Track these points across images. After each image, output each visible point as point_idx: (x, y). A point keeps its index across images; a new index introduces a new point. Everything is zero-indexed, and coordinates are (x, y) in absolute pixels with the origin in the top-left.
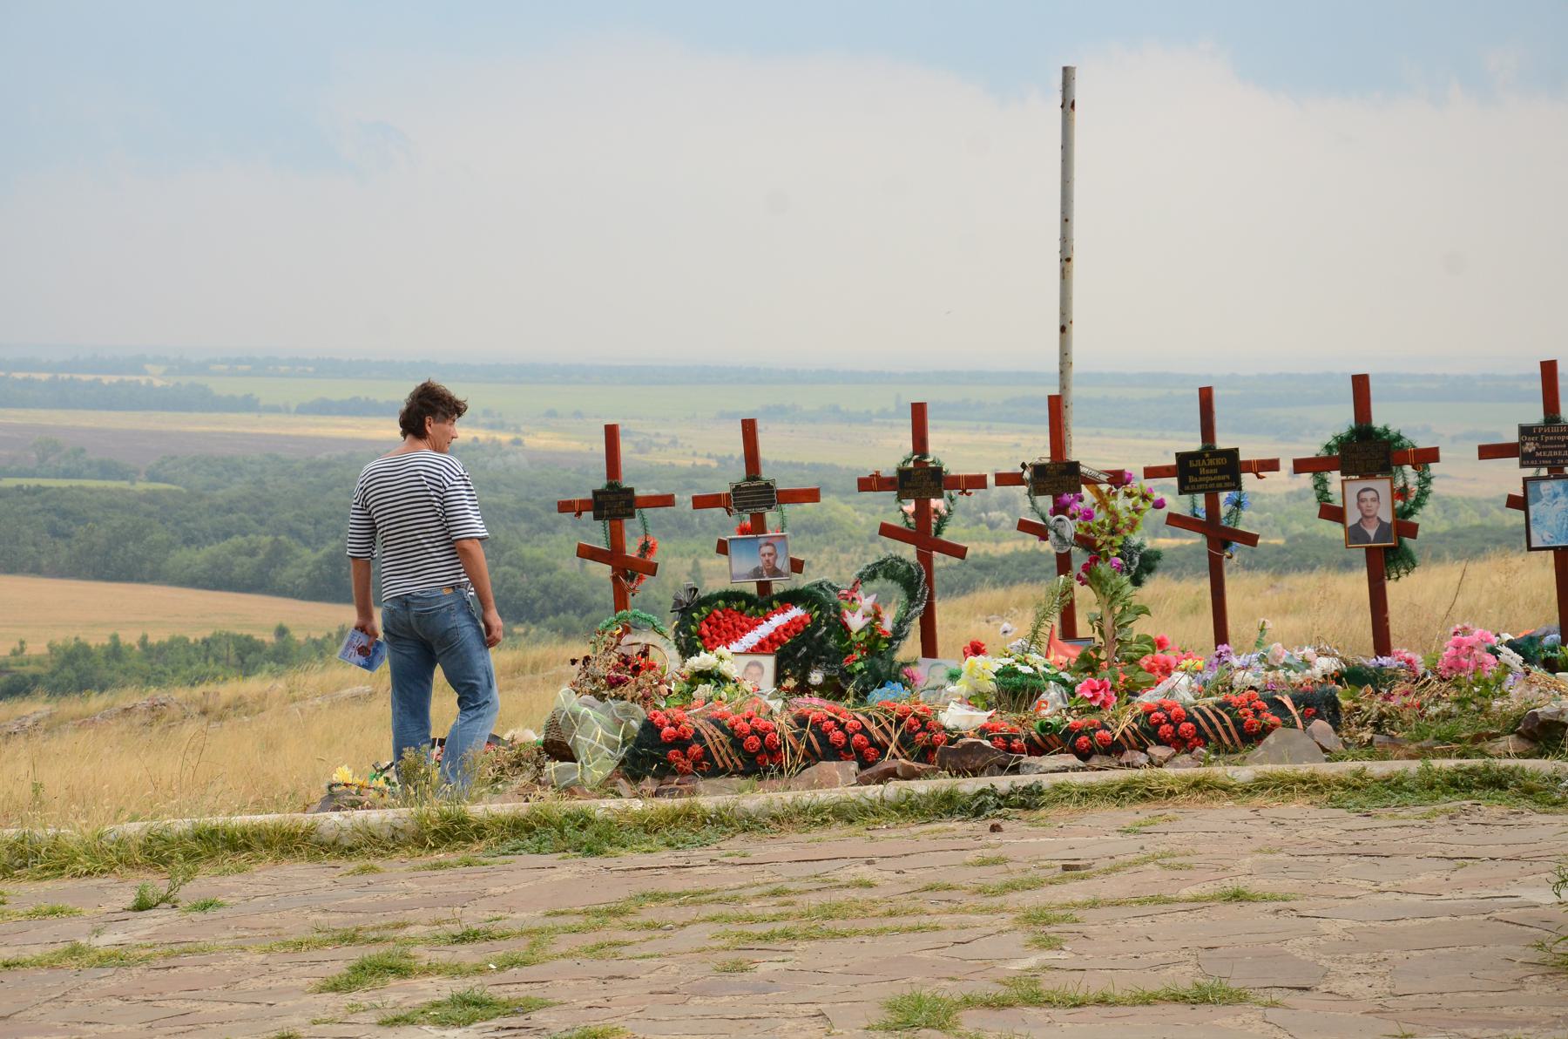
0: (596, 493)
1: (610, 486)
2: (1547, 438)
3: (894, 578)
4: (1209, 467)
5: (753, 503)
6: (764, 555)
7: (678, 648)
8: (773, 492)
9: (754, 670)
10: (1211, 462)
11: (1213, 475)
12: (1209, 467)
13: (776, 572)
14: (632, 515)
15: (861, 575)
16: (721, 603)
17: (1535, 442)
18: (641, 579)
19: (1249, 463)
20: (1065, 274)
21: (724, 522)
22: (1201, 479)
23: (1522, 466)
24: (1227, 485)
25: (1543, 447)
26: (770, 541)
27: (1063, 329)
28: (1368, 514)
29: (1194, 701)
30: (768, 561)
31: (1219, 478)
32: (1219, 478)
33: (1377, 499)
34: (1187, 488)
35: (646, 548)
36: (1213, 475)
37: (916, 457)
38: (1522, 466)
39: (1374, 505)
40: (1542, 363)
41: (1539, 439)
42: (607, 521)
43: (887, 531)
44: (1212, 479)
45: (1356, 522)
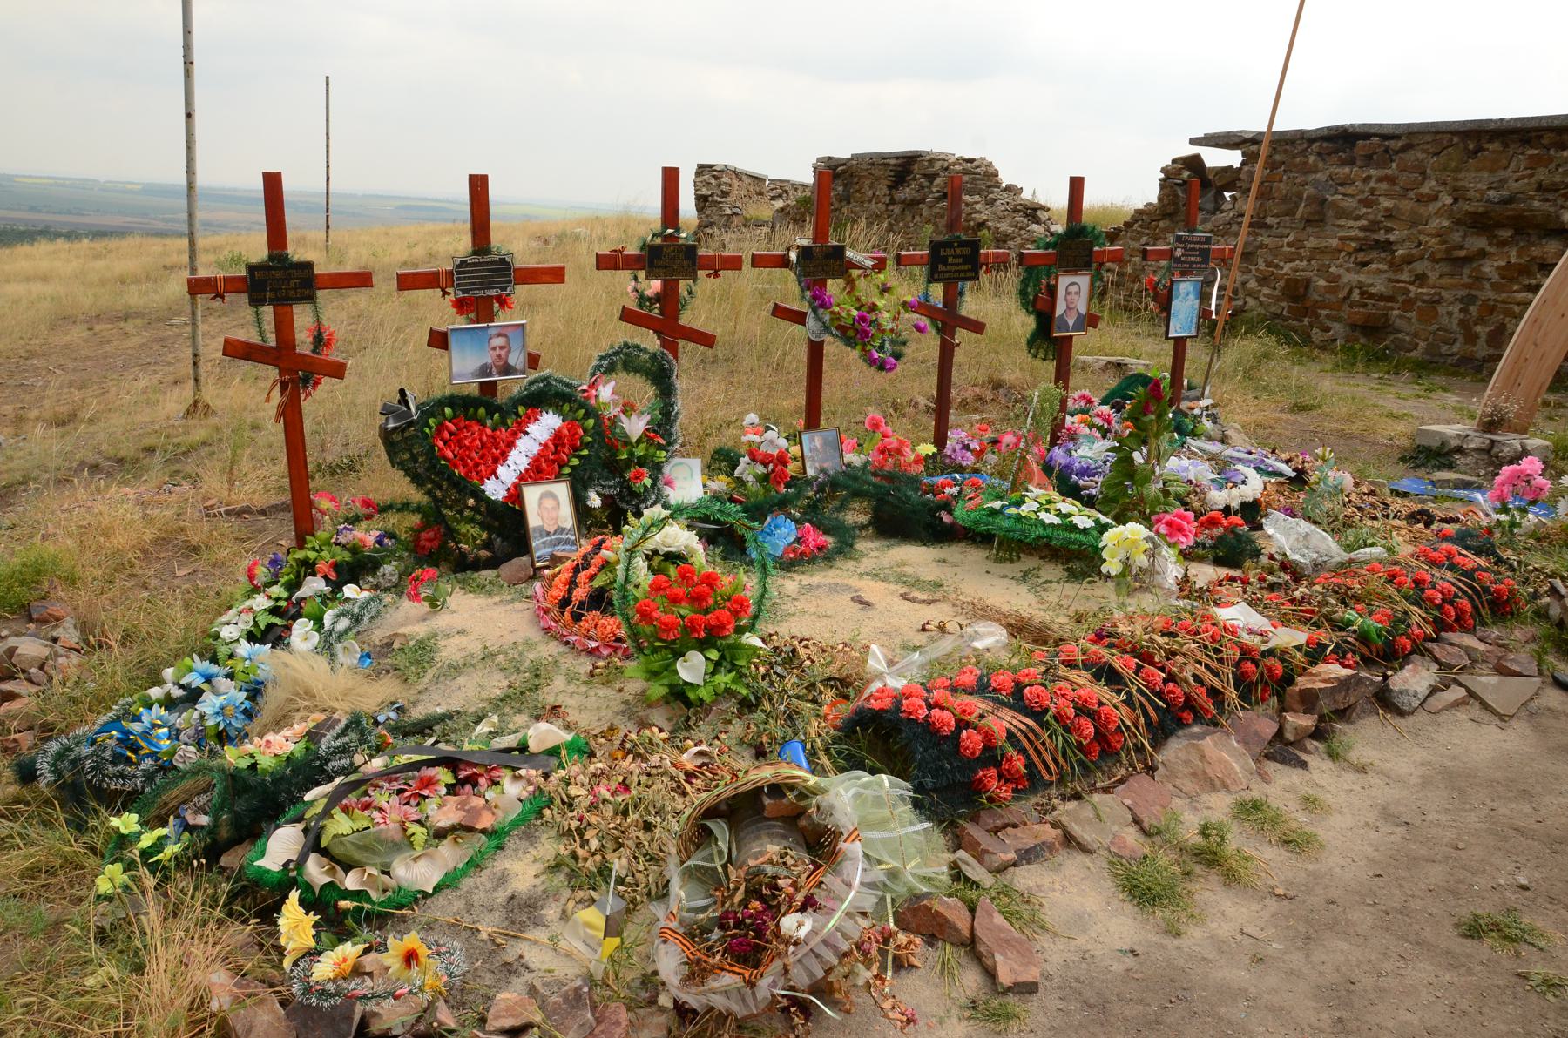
0: (252, 268)
1: (271, 258)
3: (636, 370)
4: (955, 257)
5: (482, 283)
6: (494, 349)
7: (407, 474)
8: (510, 269)
9: (549, 503)
10: (958, 251)
11: (958, 265)
12: (955, 257)
13: (507, 369)
14: (311, 298)
15: (598, 367)
16: (448, 410)
18: (316, 384)
20: (188, 74)
21: (437, 309)
22: (949, 268)
24: (969, 274)
26: (504, 331)
27: (189, 116)
29: (1346, 556)
30: (499, 356)
31: (962, 267)
32: (962, 267)
33: (1078, 293)
34: (936, 276)
35: (320, 340)
36: (958, 265)
37: (670, 231)
42: (268, 311)
43: (627, 316)
44: (956, 268)
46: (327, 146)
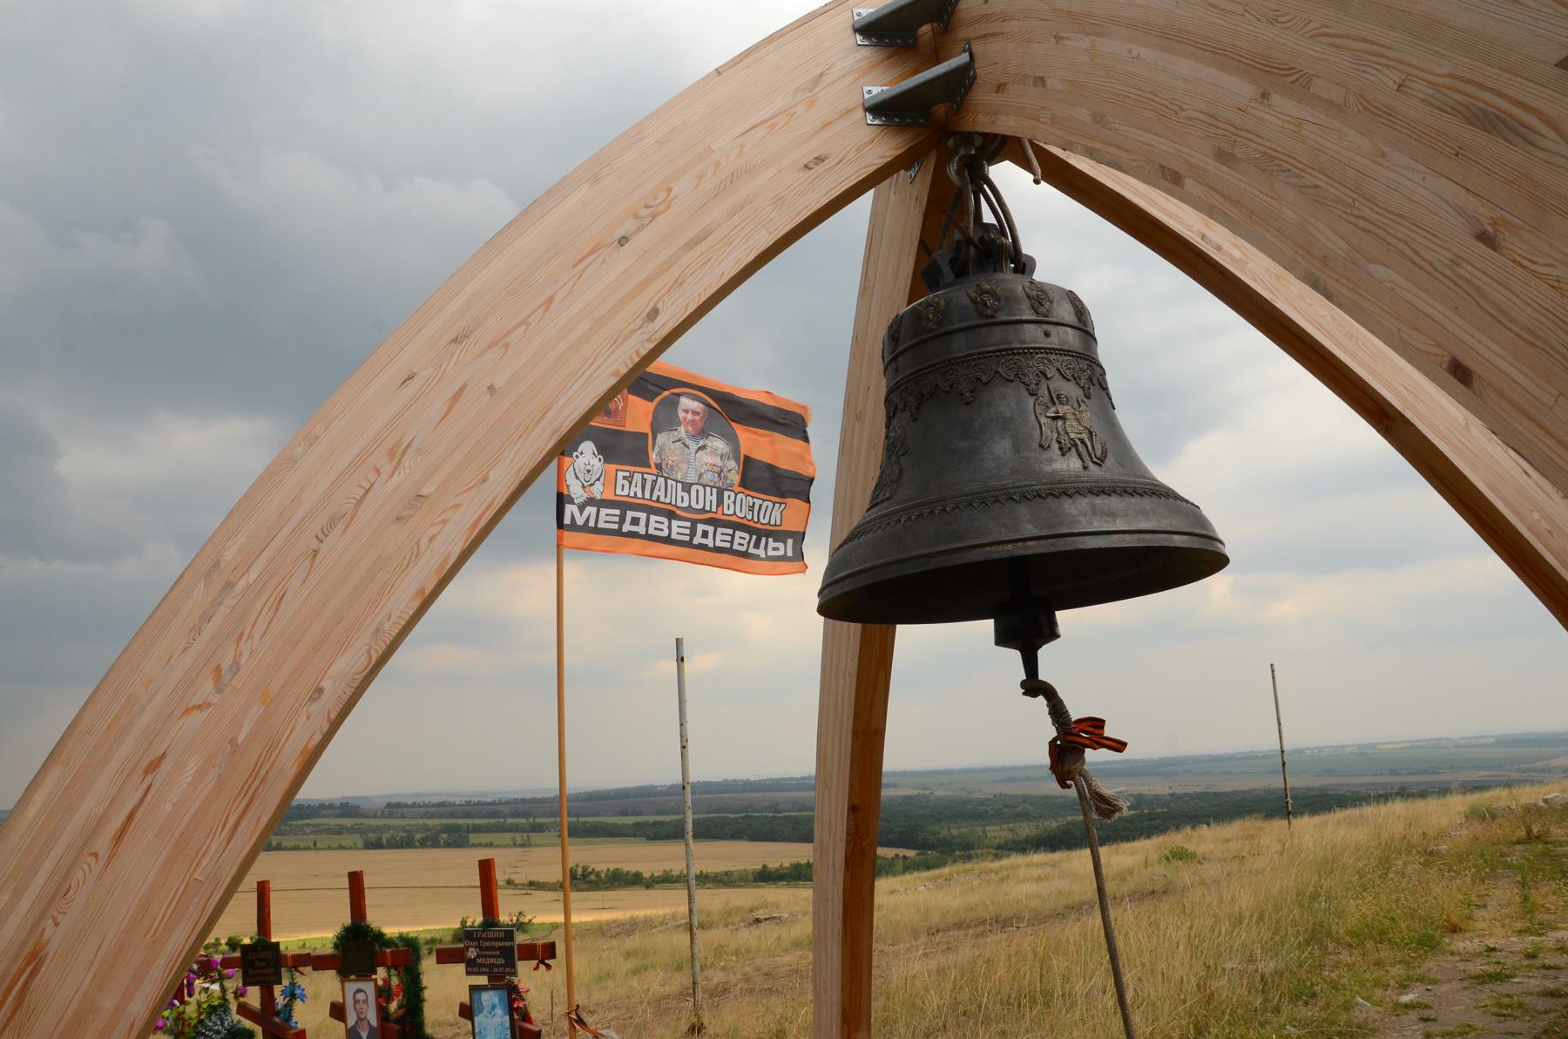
2: (485, 943)
17: (476, 947)
19: (286, 956)
23: (468, 973)
25: (484, 953)
28: (363, 1016)
33: (366, 1001)
38: (468, 973)
39: (364, 1006)
40: (480, 861)
41: (479, 944)
45: (353, 1023)
46: (1280, 732)
